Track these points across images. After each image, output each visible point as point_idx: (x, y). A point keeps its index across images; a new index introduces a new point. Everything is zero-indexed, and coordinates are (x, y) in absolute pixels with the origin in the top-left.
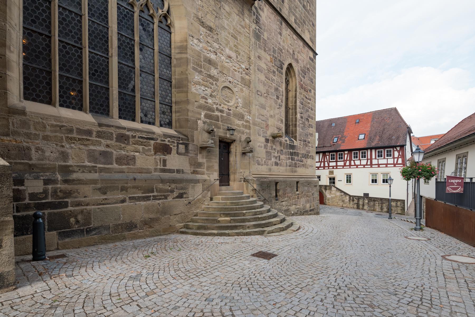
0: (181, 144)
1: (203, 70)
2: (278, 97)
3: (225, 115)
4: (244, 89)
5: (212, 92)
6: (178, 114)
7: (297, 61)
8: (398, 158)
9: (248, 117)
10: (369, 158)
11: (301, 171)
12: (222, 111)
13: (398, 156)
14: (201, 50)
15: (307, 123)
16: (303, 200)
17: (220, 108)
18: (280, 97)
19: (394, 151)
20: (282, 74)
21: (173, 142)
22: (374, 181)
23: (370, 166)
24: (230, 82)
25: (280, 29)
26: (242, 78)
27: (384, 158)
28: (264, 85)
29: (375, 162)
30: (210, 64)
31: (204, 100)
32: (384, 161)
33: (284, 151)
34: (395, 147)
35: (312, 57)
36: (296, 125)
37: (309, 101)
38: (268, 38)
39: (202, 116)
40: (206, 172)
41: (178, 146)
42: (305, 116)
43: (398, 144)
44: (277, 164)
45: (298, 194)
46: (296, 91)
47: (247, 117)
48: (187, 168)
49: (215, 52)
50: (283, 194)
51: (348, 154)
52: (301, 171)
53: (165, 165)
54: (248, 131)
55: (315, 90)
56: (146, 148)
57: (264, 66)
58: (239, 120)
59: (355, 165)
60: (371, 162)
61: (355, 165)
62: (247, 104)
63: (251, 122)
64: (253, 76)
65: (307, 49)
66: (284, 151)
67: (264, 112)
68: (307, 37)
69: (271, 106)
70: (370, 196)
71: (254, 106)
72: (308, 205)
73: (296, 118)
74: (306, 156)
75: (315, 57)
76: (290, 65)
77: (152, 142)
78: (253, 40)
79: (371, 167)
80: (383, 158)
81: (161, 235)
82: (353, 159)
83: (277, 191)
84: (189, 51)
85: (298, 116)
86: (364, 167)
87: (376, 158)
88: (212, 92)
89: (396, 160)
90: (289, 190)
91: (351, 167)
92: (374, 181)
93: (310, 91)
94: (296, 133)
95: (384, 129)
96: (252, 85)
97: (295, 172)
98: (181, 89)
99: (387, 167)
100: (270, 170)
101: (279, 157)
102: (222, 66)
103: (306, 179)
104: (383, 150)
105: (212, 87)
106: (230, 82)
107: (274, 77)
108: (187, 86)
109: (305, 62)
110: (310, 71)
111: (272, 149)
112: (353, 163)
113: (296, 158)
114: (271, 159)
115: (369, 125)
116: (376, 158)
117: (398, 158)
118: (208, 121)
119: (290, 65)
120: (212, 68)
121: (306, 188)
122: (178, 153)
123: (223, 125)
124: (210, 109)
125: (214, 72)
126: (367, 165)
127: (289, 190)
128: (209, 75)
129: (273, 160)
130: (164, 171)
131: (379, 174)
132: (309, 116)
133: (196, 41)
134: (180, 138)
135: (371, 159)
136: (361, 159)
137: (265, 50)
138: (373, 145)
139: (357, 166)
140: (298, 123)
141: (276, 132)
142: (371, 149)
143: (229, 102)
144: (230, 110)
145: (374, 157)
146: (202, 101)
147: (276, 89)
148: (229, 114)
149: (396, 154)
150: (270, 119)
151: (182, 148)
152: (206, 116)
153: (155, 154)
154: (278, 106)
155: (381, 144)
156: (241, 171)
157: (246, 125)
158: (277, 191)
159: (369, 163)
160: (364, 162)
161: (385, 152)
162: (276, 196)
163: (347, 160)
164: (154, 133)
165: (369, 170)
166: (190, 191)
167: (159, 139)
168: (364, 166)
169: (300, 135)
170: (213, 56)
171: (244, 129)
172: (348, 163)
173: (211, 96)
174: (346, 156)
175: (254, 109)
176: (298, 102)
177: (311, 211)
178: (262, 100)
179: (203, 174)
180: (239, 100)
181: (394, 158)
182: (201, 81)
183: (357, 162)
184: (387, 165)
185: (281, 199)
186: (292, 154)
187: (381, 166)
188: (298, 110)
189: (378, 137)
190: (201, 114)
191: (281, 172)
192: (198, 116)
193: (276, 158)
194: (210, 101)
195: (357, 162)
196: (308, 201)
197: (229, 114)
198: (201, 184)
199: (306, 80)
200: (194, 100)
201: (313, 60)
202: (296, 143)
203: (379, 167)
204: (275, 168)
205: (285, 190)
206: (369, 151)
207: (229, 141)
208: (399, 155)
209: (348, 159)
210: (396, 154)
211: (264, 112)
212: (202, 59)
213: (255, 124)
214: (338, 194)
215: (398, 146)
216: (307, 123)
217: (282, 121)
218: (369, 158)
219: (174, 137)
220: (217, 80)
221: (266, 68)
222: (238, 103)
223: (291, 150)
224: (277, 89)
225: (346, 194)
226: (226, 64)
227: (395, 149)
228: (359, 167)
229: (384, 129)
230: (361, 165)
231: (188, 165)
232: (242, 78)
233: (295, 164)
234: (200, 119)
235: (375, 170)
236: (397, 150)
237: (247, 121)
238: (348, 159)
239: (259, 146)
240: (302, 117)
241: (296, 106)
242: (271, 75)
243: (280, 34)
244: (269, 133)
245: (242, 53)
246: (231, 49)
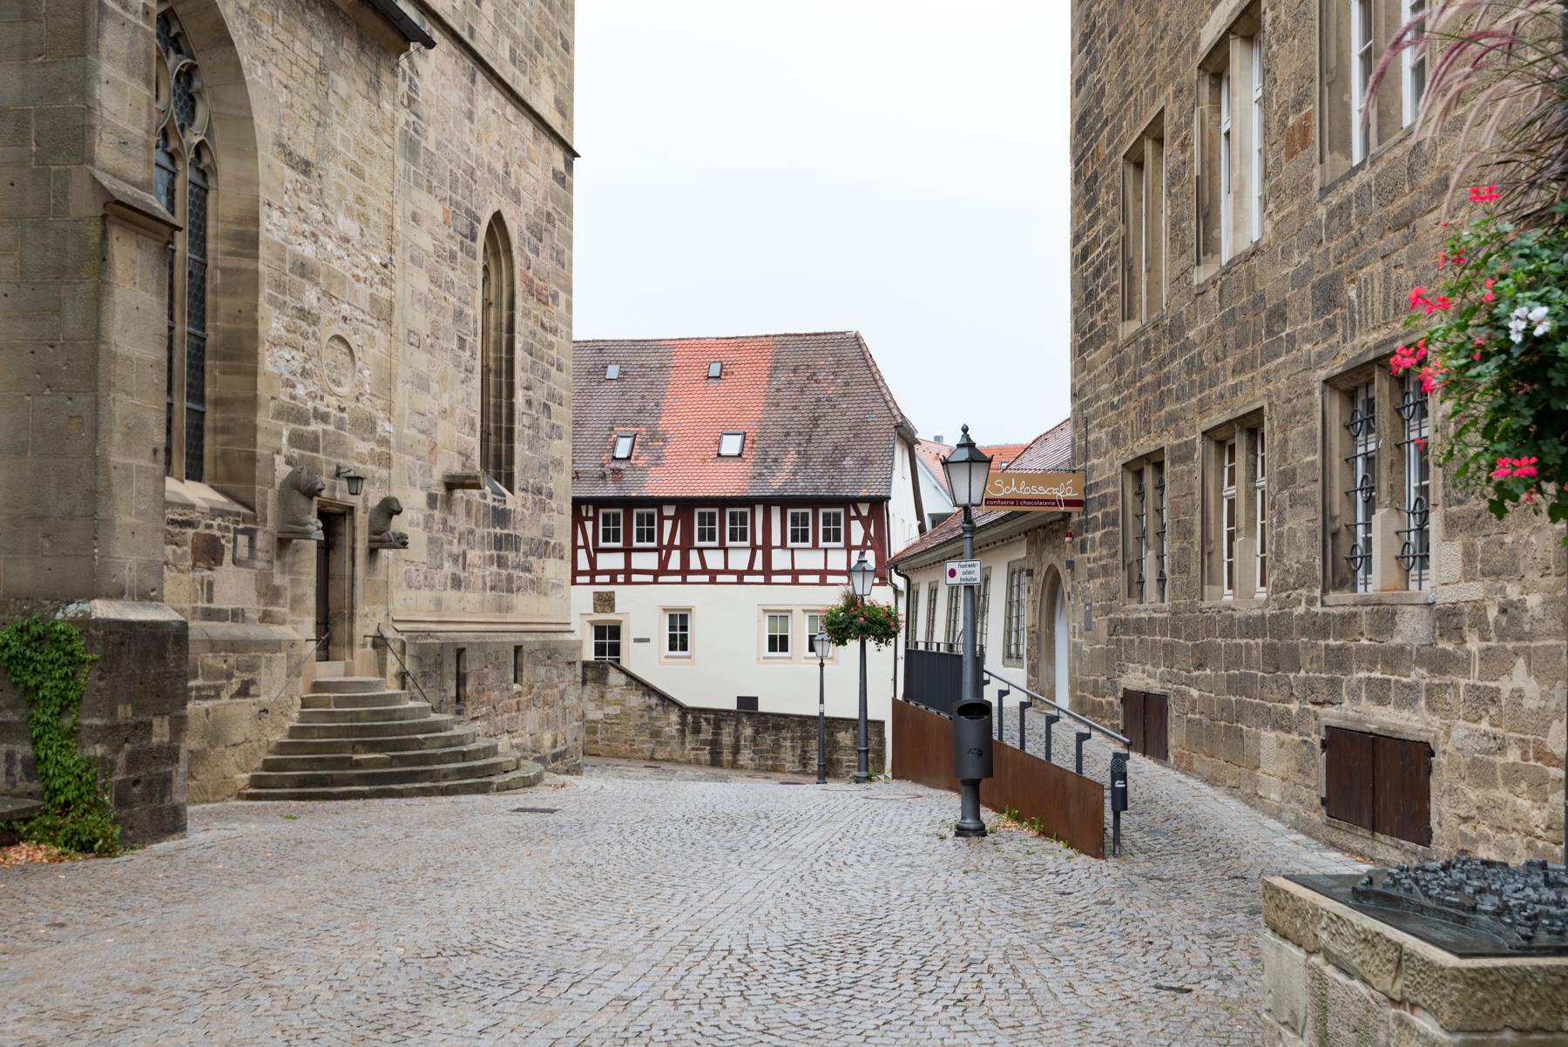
0: (243, 532)
1: (288, 298)
2: (462, 343)
3: (331, 428)
4: (377, 333)
5: (306, 361)
6: (221, 438)
7: (516, 196)
8: (863, 548)
9: (387, 424)
10: (759, 542)
11: (527, 607)
12: (324, 418)
13: (864, 541)
14: (286, 240)
15: (543, 421)
16: (532, 717)
17: (322, 408)
18: (469, 339)
19: (849, 519)
20: (474, 257)
21: (227, 529)
22: (778, 643)
23: (761, 579)
24: (345, 319)
25: (471, 101)
26: (374, 300)
27: (815, 546)
28: (428, 307)
29: (780, 560)
30: (303, 276)
31: (289, 390)
33: (479, 531)
35: (561, 167)
36: (510, 431)
37: (550, 337)
38: (439, 145)
39: (284, 440)
40: (290, 617)
41: (235, 540)
42: (539, 395)
43: (863, 493)
44: (457, 583)
45: (519, 694)
46: (512, 306)
47: (384, 427)
48: (252, 605)
49: (314, 234)
50: (477, 691)
51: (674, 519)
52: (527, 607)
53: (210, 600)
54: (383, 472)
55: (569, 291)
56: (179, 551)
57: (427, 243)
58: (363, 439)
59: (704, 570)
61: (704, 570)
62: (386, 384)
63: (392, 440)
64: (398, 286)
65: (546, 142)
66: (479, 531)
67: (426, 402)
68: (544, 105)
69: (443, 378)
70: (761, 708)
71: (400, 385)
72: (547, 738)
73: (511, 407)
74: (543, 549)
75: (569, 166)
76: (498, 218)
77: (190, 532)
78: (401, 163)
79: (768, 582)
80: (809, 544)
81: (208, 802)
82: (697, 544)
83: (461, 680)
84: (263, 251)
85: (519, 399)
86: (740, 582)
87: (783, 546)
88: (306, 361)
90: (492, 676)
91: (690, 578)
92: (778, 643)
93: (555, 296)
94: (511, 461)
96: (397, 318)
97: (509, 609)
98: (235, 363)
99: (823, 583)
100: (439, 603)
101: (464, 554)
102: (331, 275)
103: (542, 638)
104: (809, 511)
105: (306, 343)
106: (345, 319)
107: (452, 275)
108: (253, 356)
109: (540, 195)
110: (555, 218)
111: (444, 530)
112: (695, 563)
113: (511, 556)
114: (440, 567)
116: (783, 546)
118: (296, 453)
119: (498, 218)
120: (308, 285)
121: (542, 671)
122: (235, 562)
123: (329, 463)
124: (299, 417)
125: (311, 297)
127: (492, 676)
128: (301, 310)
129: (448, 568)
130: (210, 615)
131: (797, 612)
132: (551, 396)
133: (276, 214)
134: (238, 514)
135: (767, 548)
136: (728, 543)
137: (430, 190)
138: (776, 484)
139: (713, 574)
140: (517, 427)
141: (457, 469)
143: (339, 384)
144: (342, 410)
145: (776, 541)
146: (284, 395)
147: (459, 316)
148: (340, 425)
149: (857, 532)
150: (442, 424)
151: (243, 540)
152: (297, 440)
153: (194, 566)
154: (463, 375)
155: (803, 487)
156: (367, 610)
157: (380, 454)
158: (461, 680)
159: (758, 566)
160: (739, 560)
162: (458, 698)
163: (671, 547)
164: (192, 507)
165: (757, 596)
166: (263, 677)
167: (203, 522)
168: (740, 574)
169: (525, 469)
170: (308, 250)
171: (373, 468)
172: (675, 562)
173: (305, 373)
174: (668, 525)
175: (402, 393)
176: (518, 346)
177: (555, 757)
178: (420, 359)
179: (282, 623)
180: (366, 373)
181: (849, 548)
182: (283, 332)
183: (714, 560)
184: (824, 574)
185: (470, 711)
186: (499, 543)
187: (802, 579)
188: (520, 377)
189: (792, 456)
190: (279, 435)
191: (466, 612)
192: (274, 442)
193: (456, 560)
194: (300, 391)
195: (714, 560)
196: (546, 722)
197: (340, 425)
198: (284, 654)
199: (544, 262)
200: (268, 396)
201: (563, 179)
202: (513, 502)
203: (795, 582)
204: (451, 595)
205: (481, 678)
207: (337, 510)
208: (867, 536)
209: (677, 542)
210: (857, 532)
211: (426, 402)
212: (288, 266)
213: (401, 448)
214: (636, 700)
215: (863, 500)
216: (543, 421)
217: (473, 425)
218: (759, 542)
219: (229, 513)
220: (315, 321)
221: (431, 249)
222: (362, 384)
223: (498, 530)
224: (461, 313)
225: (666, 701)
226: (336, 265)
227: (853, 513)
228: (720, 578)
229: (815, 420)
230: (726, 571)
231: (253, 595)
232: (374, 300)
233: (510, 578)
234: (278, 452)
235: (781, 595)
236: (859, 517)
237: (384, 442)
238: (677, 542)
239: (411, 523)
240: (529, 403)
241: (511, 362)
242: (446, 270)
243: (470, 116)
244: (438, 474)
245: (374, 217)
246: (349, 212)
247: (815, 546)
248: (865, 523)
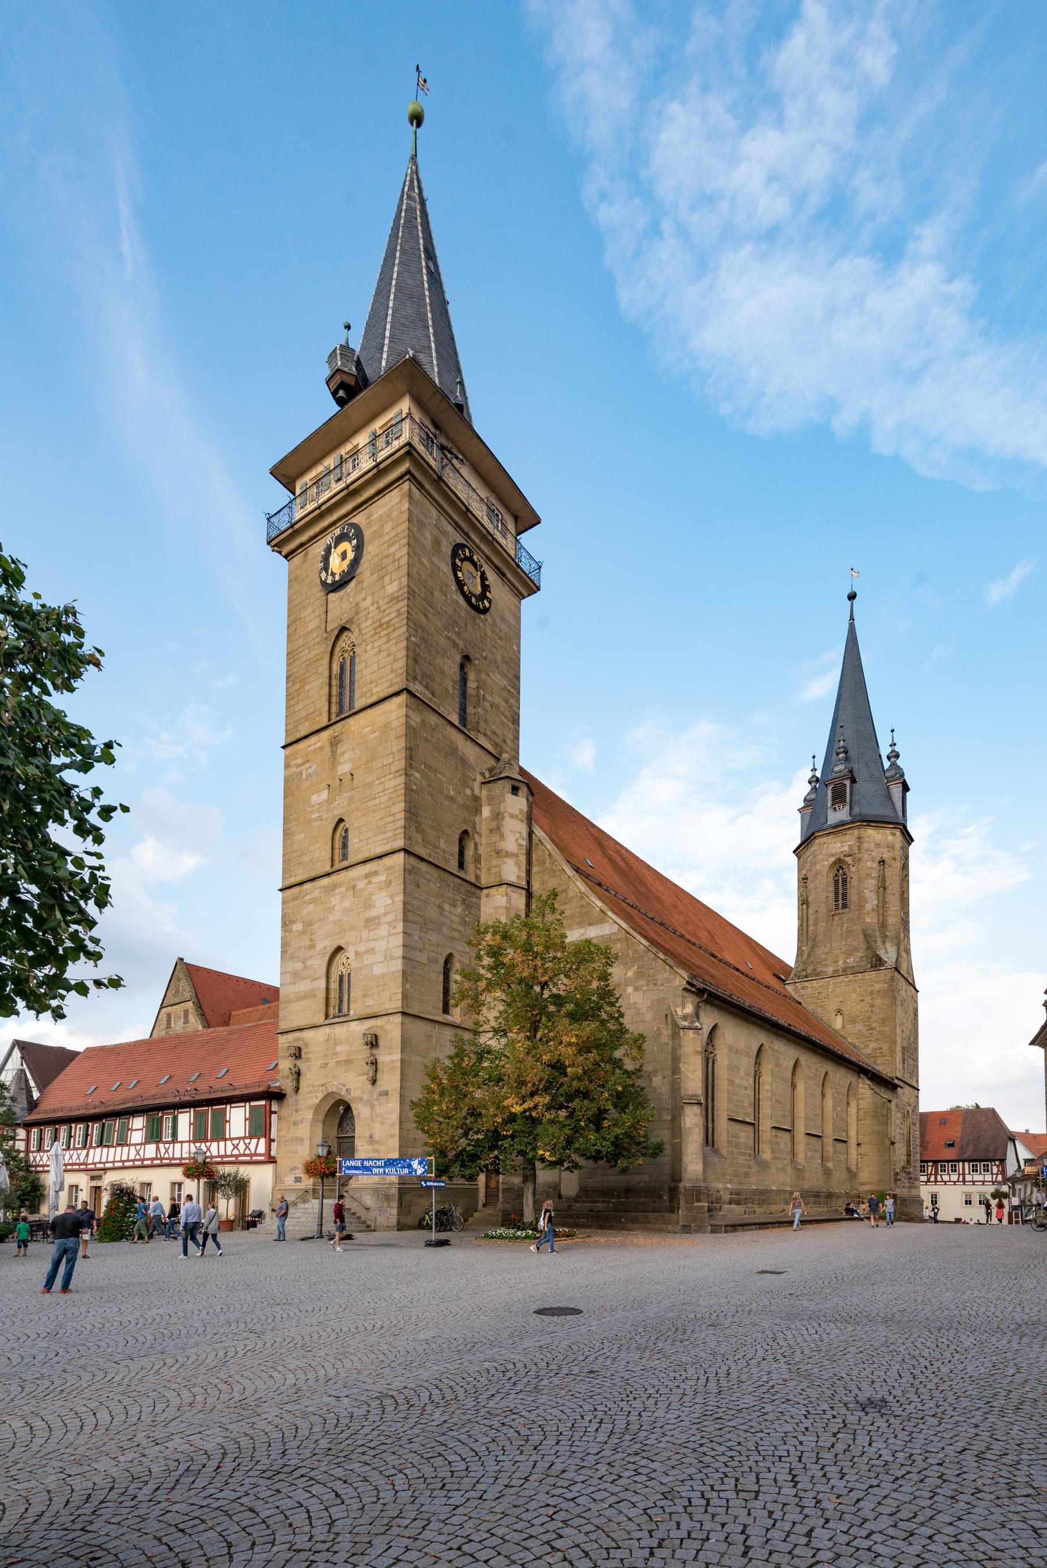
29: (968, 1178)
32: (981, 1178)
34: (994, 1160)
60: (964, 1178)
112: (939, 1179)
115: (959, 1128)
135: (964, 1174)
138: (966, 1156)
139: (945, 1182)
142: (964, 1161)
145: (967, 1172)
155: (976, 1157)
160: (954, 1178)
161: (981, 1166)
165: (960, 1189)
172: (932, 1178)
181: (992, 1174)
184: (983, 1182)
189: (971, 1147)
195: (946, 1178)
235: (969, 1188)
248: (998, 1167)
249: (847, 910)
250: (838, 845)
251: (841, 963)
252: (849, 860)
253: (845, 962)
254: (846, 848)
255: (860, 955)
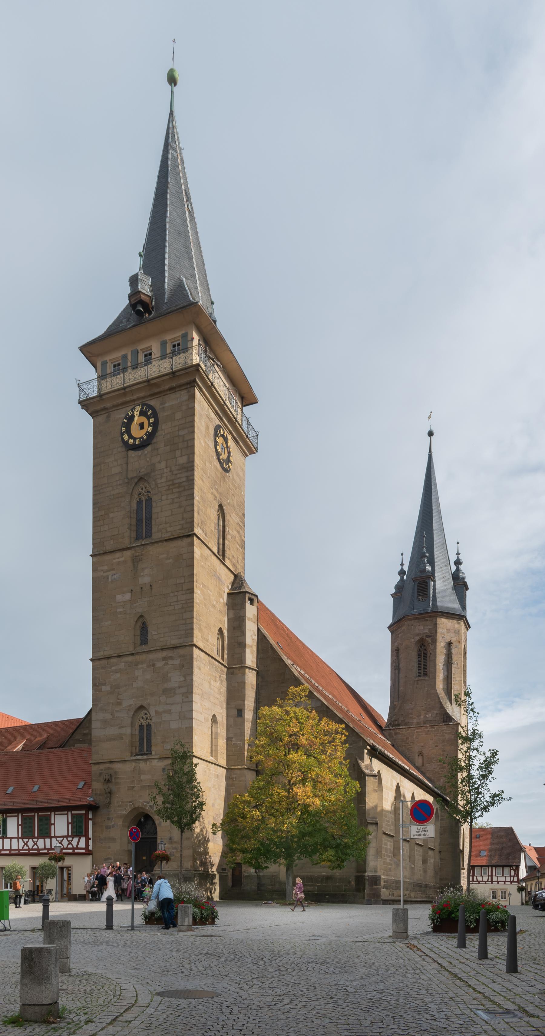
8: (514, 876)
29: (495, 879)
32: (502, 879)
59: (477, 881)
60: (492, 879)
79: (492, 883)
87: (495, 875)
89: (512, 878)
95: (502, 848)
99: (505, 884)
112: (475, 879)
116: (495, 875)
117: (514, 876)
126: (488, 881)
135: (492, 876)
139: (479, 882)
142: (492, 866)
145: (494, 874)
155: (500, 863)
159: (490, 880)
160: (485, 879)
168: (485, 882)
184: (505, 882)
195: (480, 879)
203: (498, 883)
206: (490, 868)
208: (515, 874)
230: (482, 881)
235: (495, 886)
236: (513, 869)
247: (503, 875)
248: (515, 871)
249: (427, 678)
250: (422, 628)
251: (422, 717)
252: (429, 640)
253: (425, 717)
254: (427, 631)
255: (435, 712)
